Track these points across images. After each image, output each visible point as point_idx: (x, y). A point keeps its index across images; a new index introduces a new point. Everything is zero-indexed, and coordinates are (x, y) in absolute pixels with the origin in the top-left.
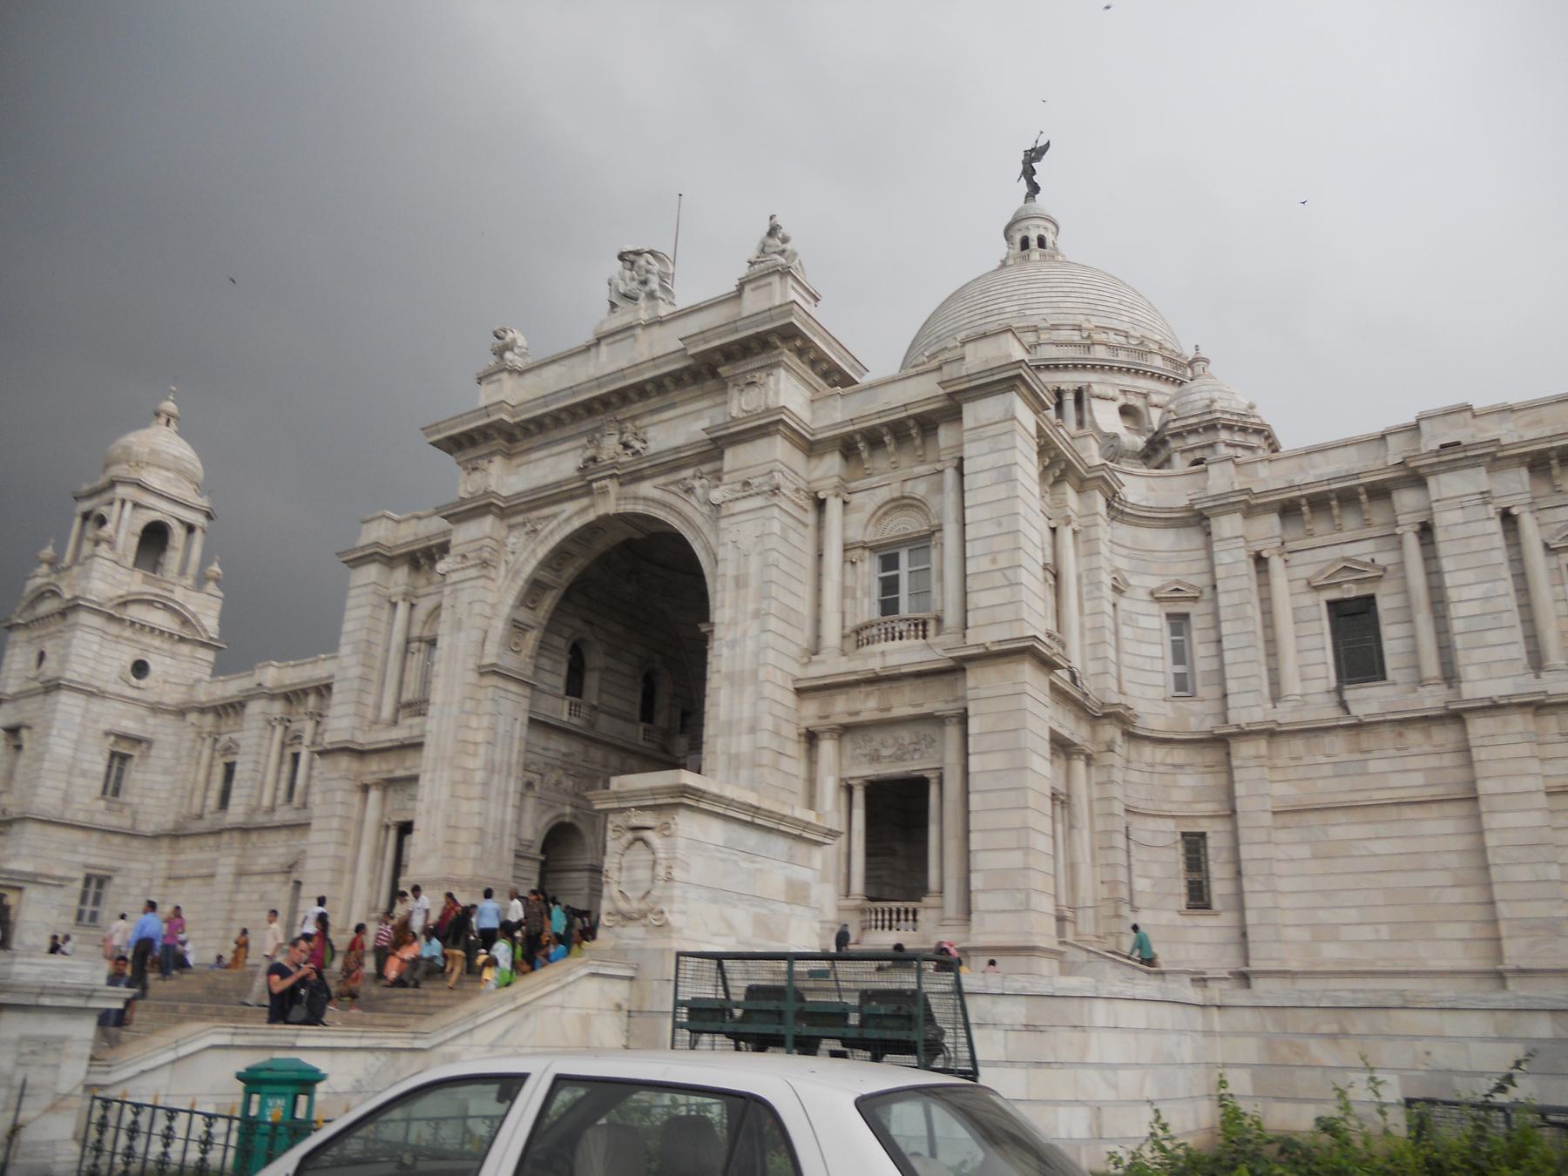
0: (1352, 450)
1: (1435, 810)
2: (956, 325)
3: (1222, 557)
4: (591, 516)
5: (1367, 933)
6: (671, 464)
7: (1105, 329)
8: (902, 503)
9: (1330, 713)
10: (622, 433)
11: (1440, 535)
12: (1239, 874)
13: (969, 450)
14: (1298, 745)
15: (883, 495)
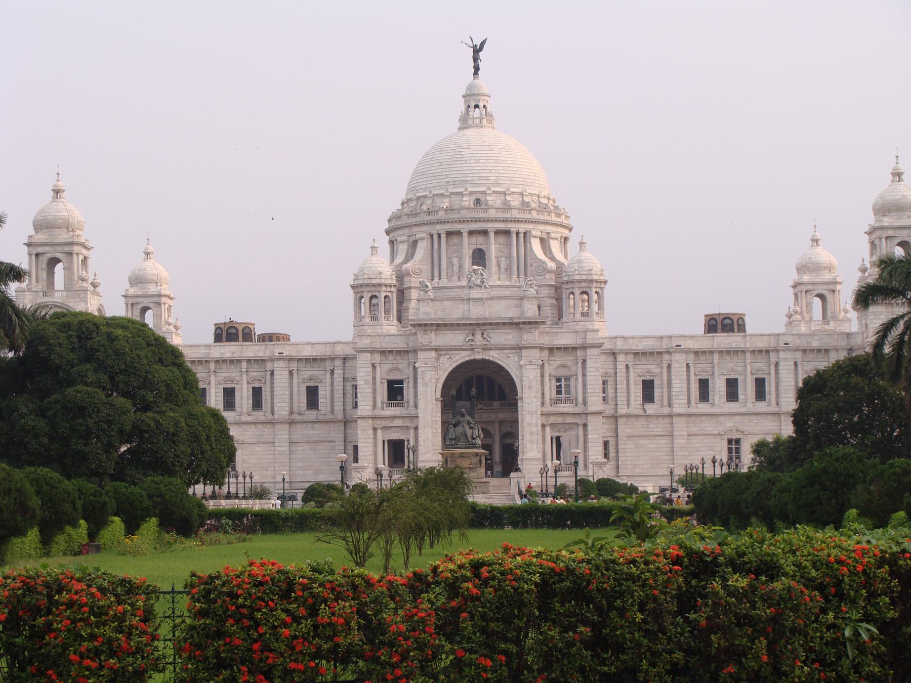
0: (654, 340)
1: (663, 438)
2: (464, 179)
3: (619, 366)
4: (472, 357)
5: (645, 466)
6: (501, 348)
7: (531, 195)
8: (563, 366)
9: (641, 412)
10: (482, 334)
11: (673, 369)
12: (617, 452)
13: (588, 361)
14: (633, 419)
15: (559, 363)
